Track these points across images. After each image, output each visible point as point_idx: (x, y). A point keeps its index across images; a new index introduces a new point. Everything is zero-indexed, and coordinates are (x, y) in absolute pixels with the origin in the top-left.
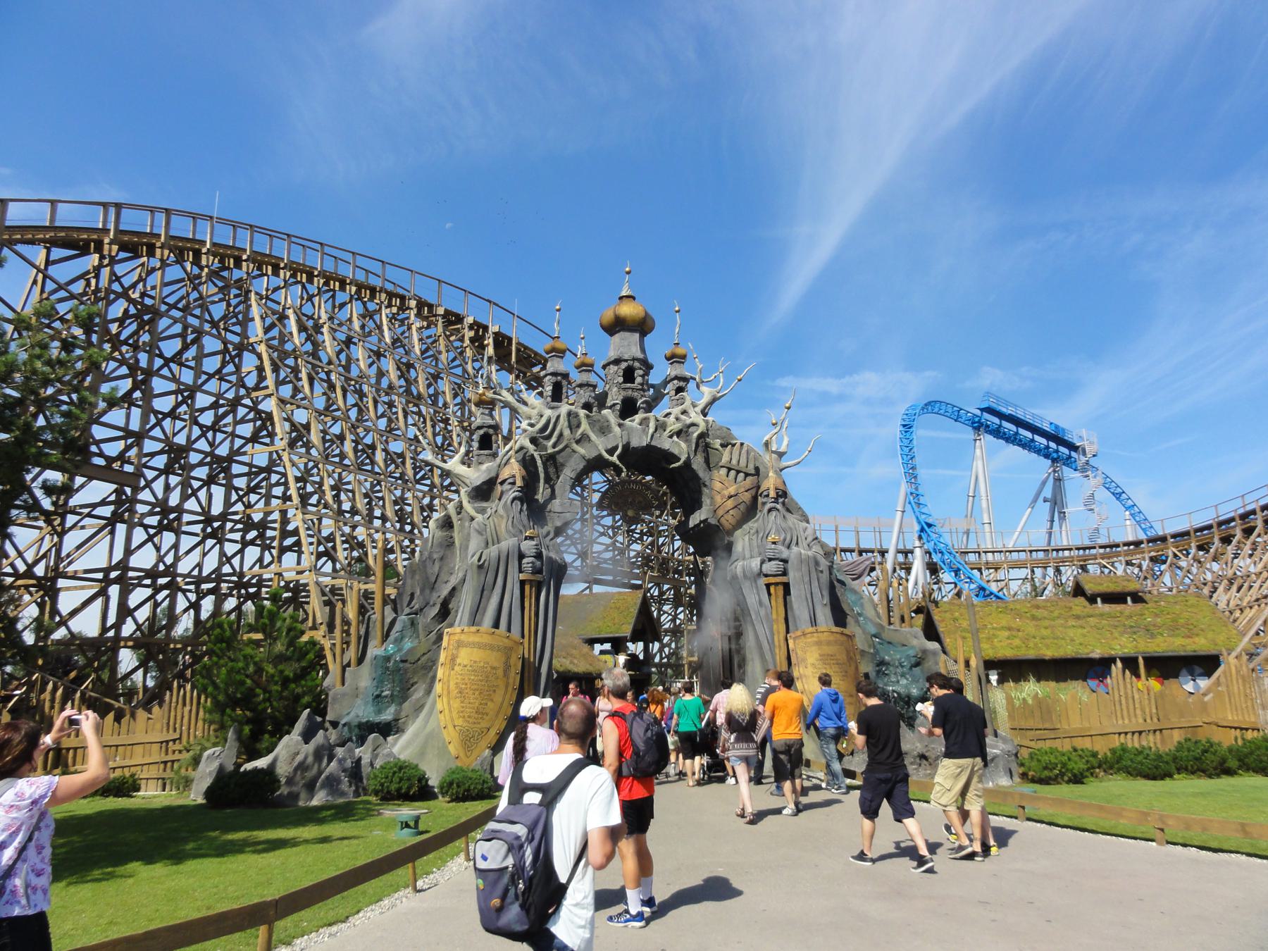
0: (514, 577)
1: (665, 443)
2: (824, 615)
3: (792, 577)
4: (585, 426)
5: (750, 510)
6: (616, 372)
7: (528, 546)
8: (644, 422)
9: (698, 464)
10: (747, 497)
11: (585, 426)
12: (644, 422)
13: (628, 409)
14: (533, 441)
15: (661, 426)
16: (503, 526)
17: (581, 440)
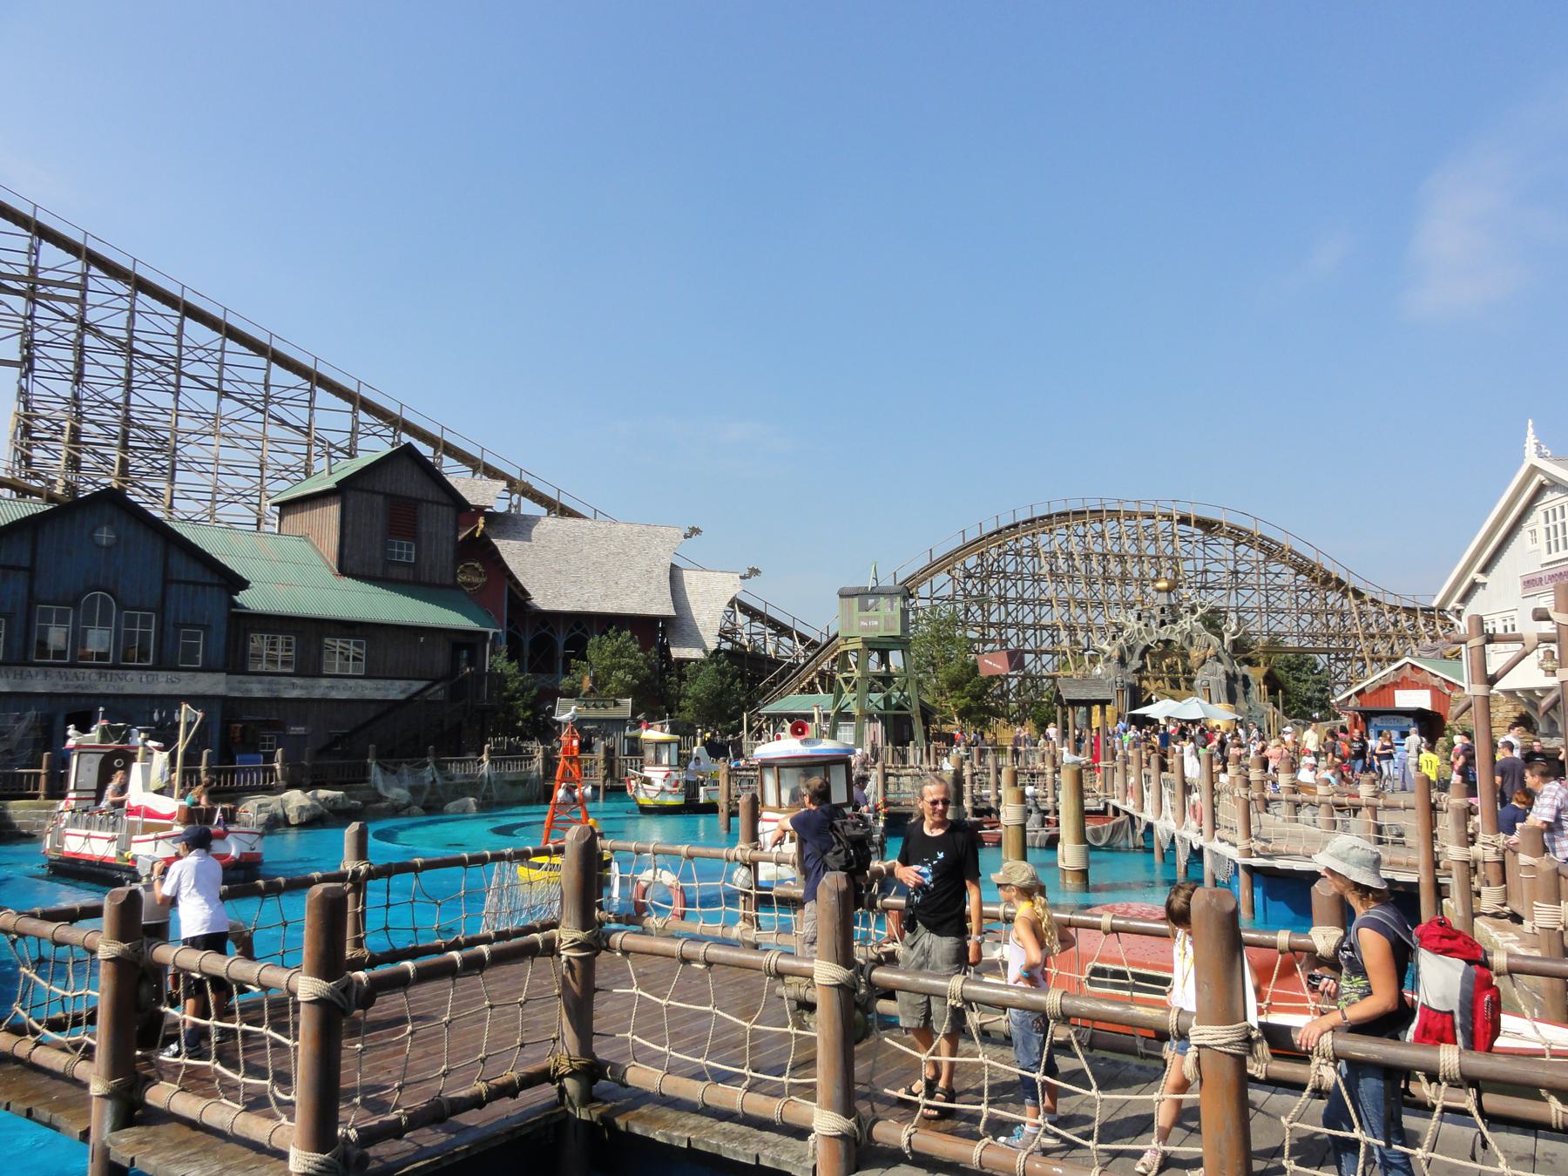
0: (1115, 689)
1: (1173, 637)
2: (1224, 697)
3: (1211, 687)
4: (1144, 633)
5: (1204, 662)
6: (1159, 608)
7: (1119, 679)
8: (1167, 629)
9: (1186, 644)
10: (1202, 657)
11: (1144, 633)
12: (1167, 629)
13: (1163, 623)
14: (1125, 640)
15: (1173, 630)
16: (1112, 672)
17: (1143, 638)
